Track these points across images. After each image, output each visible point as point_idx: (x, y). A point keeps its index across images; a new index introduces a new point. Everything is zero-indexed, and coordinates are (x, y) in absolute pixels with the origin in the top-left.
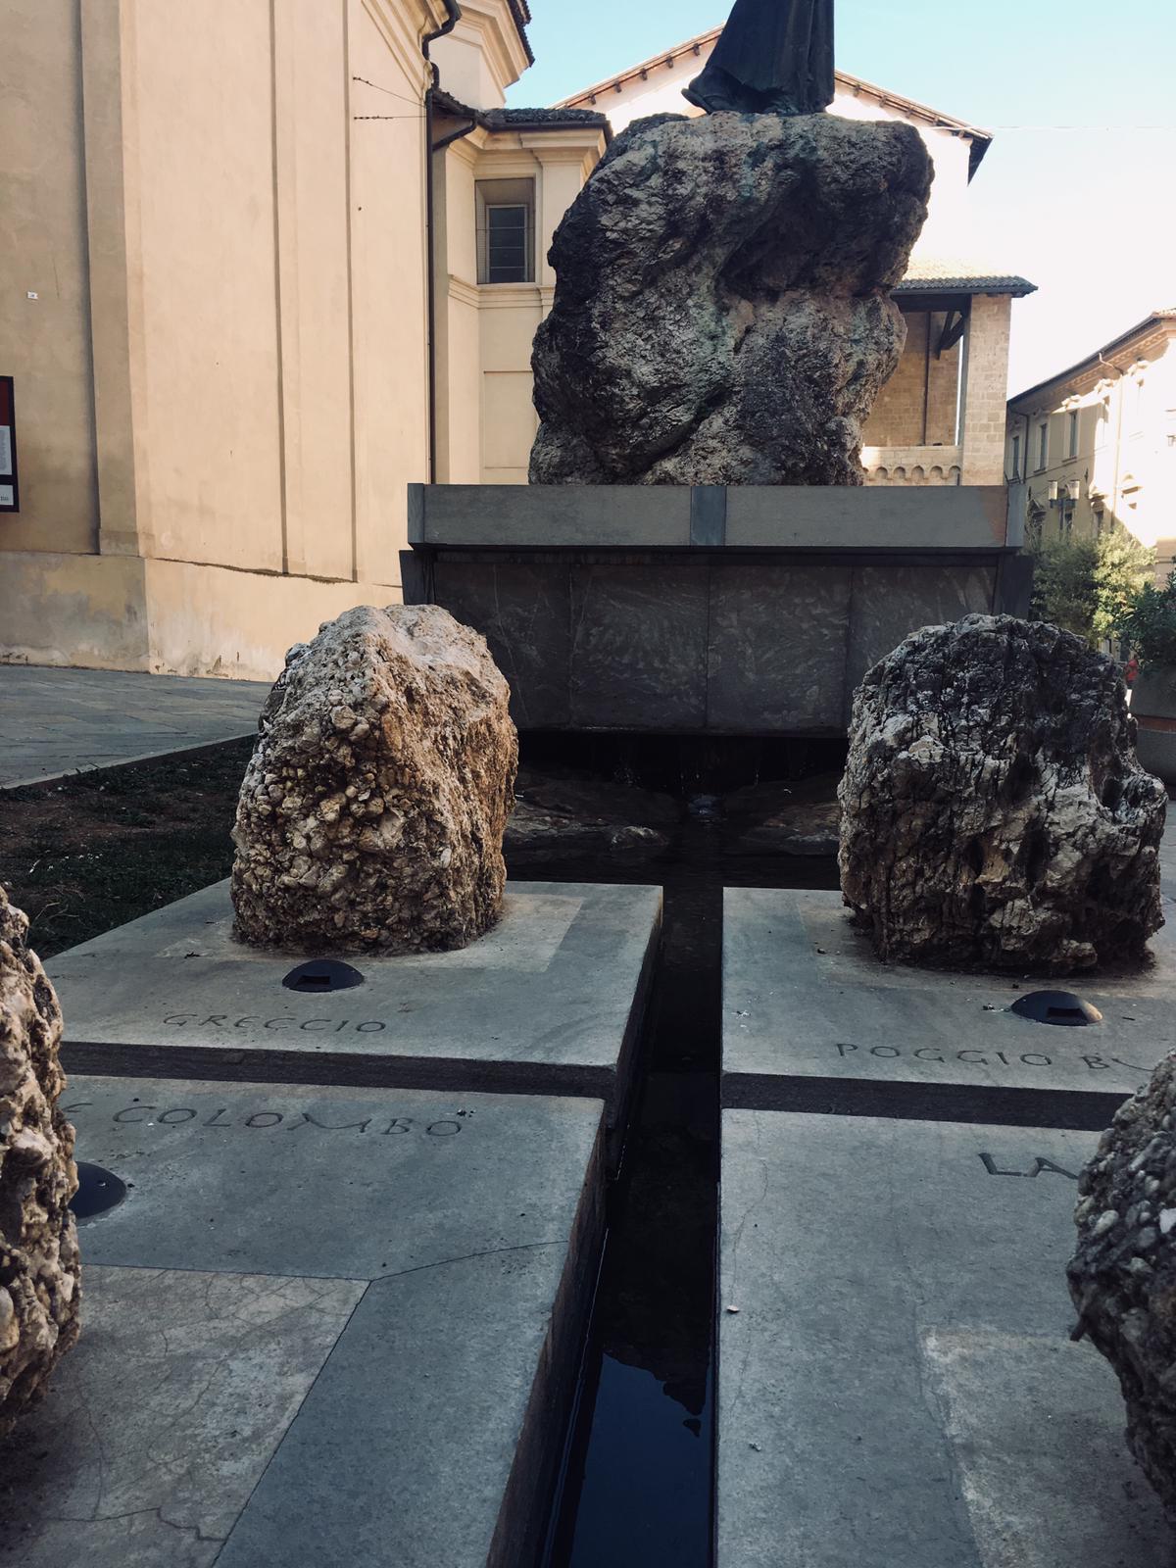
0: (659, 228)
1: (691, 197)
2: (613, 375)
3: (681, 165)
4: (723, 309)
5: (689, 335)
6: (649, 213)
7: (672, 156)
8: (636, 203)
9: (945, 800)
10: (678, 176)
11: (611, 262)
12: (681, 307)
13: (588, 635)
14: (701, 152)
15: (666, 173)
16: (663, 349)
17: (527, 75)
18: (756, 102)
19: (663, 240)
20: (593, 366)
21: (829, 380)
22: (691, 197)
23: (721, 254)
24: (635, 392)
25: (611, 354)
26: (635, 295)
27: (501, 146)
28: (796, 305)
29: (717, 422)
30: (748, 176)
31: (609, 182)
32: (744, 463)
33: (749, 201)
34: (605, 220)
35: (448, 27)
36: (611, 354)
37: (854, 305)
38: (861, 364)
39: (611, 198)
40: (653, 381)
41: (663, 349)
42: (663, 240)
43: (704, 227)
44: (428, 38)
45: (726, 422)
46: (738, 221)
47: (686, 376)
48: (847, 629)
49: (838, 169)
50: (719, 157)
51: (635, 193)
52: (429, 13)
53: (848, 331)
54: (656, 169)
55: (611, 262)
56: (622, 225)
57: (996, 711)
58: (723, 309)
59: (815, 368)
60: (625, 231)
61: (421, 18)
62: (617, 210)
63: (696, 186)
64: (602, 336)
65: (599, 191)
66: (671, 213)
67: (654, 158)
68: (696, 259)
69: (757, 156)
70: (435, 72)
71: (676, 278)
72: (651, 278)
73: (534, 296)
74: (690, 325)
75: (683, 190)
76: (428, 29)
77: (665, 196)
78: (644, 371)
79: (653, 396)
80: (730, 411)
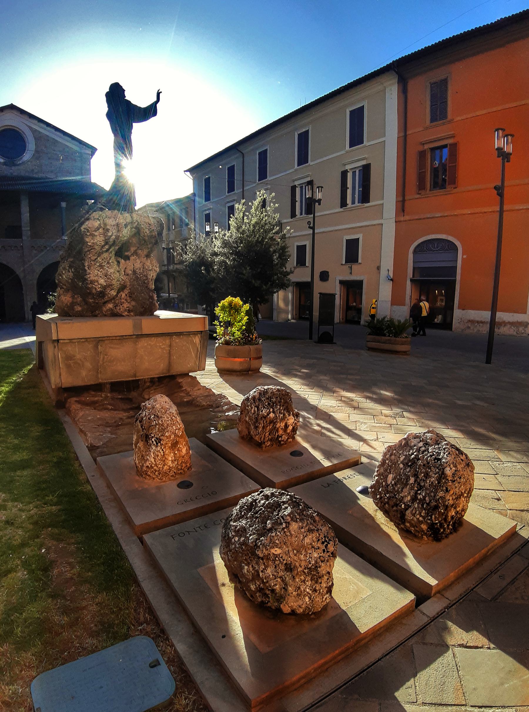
1: (111, 236)
2: (92, 282)
3: (108, 227)
6: (99, 239)
7: (105, 225)
8: (95, 236)
9: (274, 423)
10: (108, 230)
11: (89, 251)
13: (104, 358)
15: (104, 229)
19: (103, 247)
20: (86, 279)
22: (111, 236)
23: (117, 248)
24: (99, 286)
25: (91, 276)
26: (95, 259)
31: (87, 229)
34: (87, 240)
36: (91, 276)
39: (88, 234)
42: (103, 247)
45: (126, 295)
47: (114, 282)
48: (170, 350)
50: (118, 225)
51: (96, 234)
54: (101, 227)
56: (92, 241)
57: (280, 405)
58: (119, 262)
59: (145, 280)
60: (93, 243)
62: (90, 237)
65: (84, 231)
66: (106, 239)
67: (100, 225)
68: (111, 250)
69: (126, 226)
71: (105, 255)
74: (111, 268)
77: (104, 235)
79: (105, 288)
80: (126, 291)
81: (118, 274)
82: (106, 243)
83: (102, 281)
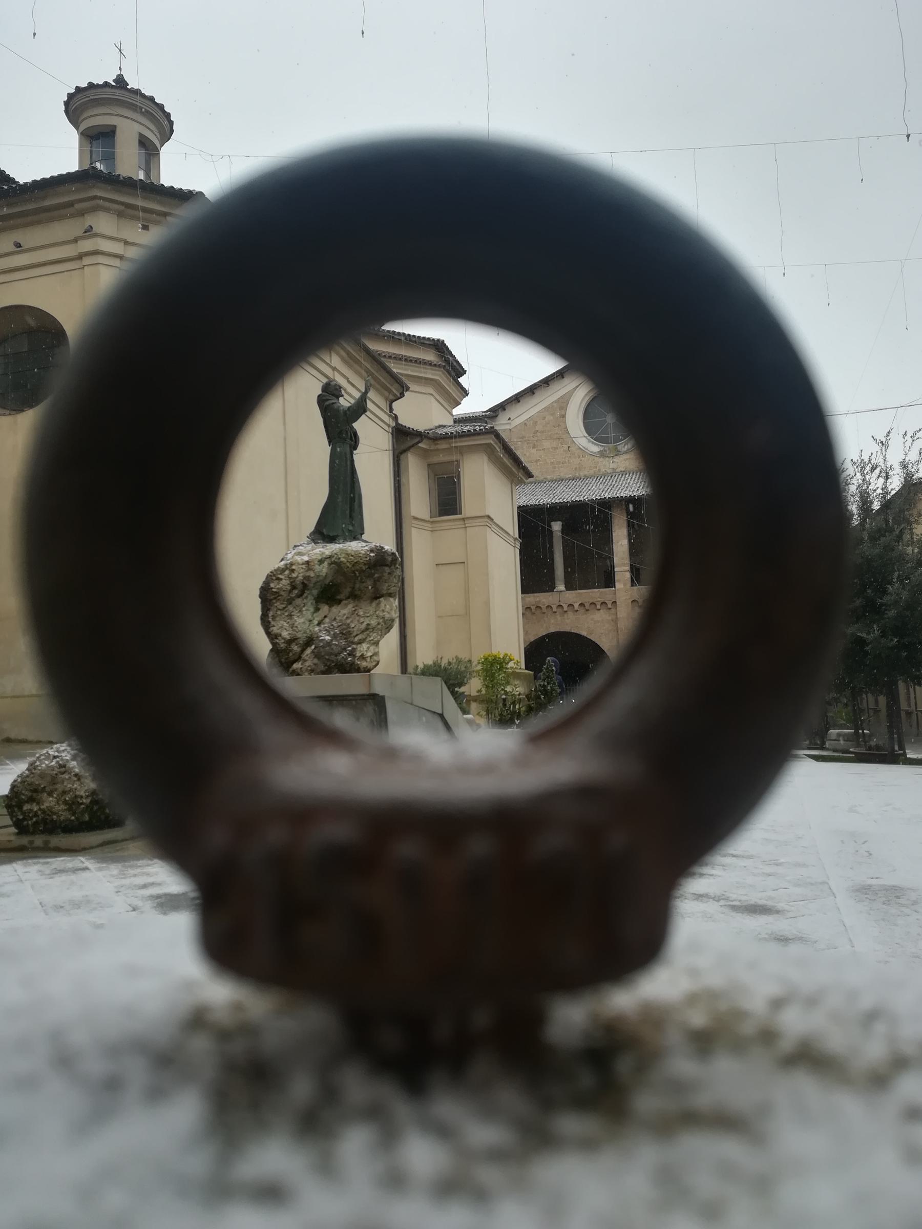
0: (289, 588)
3: (294, 567)
4: (317, 610)
5: (302, 620)
6: (285, 582)
8: (281, 579)
10: (293, 571)
11: (275, 598)
12: (300, 611)
14: (301, 562)
16: (292, 626)
17: (465, 401)
18: (331, 539)
19: (290, 591)
21: (350, 633)
22: (297, 577)
23: (315, 592)
25: (274, 628)
26: (284, 608)
27: (440, 447)
28: (346, 605)
29: (309, 651)
30: (317, 568)
32: (315, 664)
33: (318, 576)
34: (272, 585)
35: (402, 395)
37: (371, 602)
38: (368, 625)
40: (288, 637)
41: (292, 626)
42: (290, 591)
43: (305, 586)
44: (391, 402)
46: (316, 582)
47: (299, 635)
49: (348, 564)
51: (280, 576)
52: (390, 391)
53: (365, 613)
55: (275, 598)
58: (317, 610)
59: (344, 629)
61: (386, 393)
62: (276, 582)
63: (299, 574)
64: (273, 623)
68: (305, 595)
69: (321, 562)
70: (396, 418)
71: (298, 601)
72: (290, 602)
73: (462, 522)
75: (294, 575)
76: (391, 397)
78: (285, 634)
81: (308, 623)
82: (294, 587)
83: (285, 634)
